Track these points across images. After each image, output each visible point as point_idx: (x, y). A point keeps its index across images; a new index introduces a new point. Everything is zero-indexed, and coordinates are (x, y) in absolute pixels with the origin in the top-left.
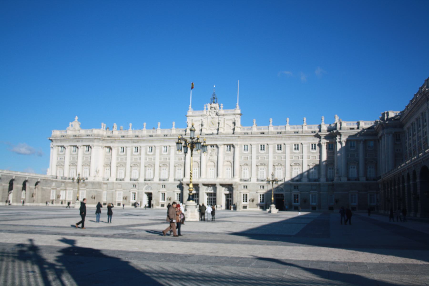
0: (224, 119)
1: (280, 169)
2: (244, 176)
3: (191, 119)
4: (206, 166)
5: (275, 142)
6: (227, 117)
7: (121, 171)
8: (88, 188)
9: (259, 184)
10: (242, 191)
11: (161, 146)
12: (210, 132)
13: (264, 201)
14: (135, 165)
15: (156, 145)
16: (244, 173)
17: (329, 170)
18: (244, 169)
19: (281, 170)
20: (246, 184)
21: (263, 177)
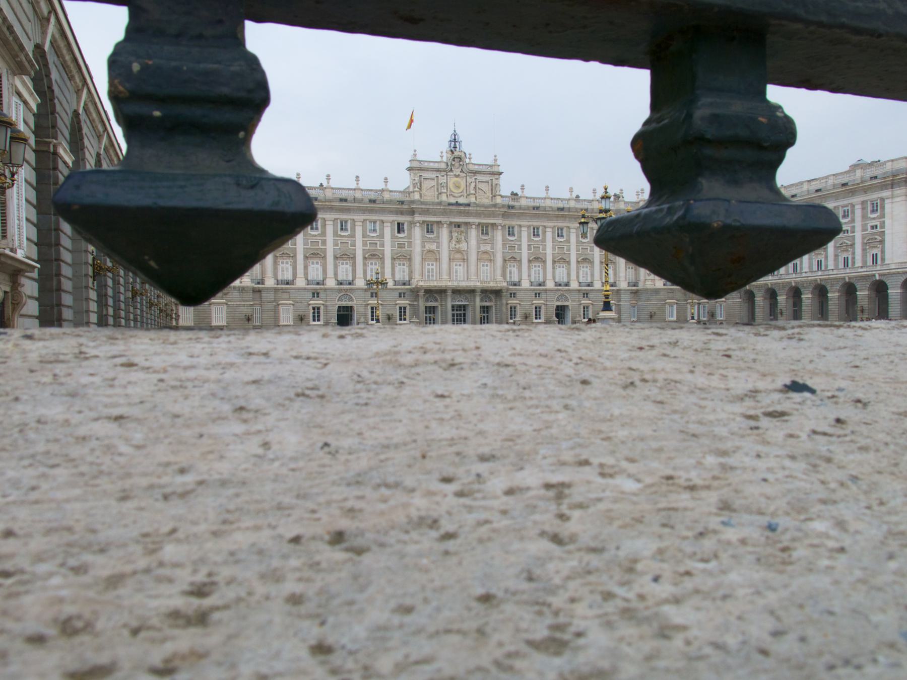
0: (476, 179)
1: (563, 267)
2: (510, 277)
3: (418, 175)
4: (450, 259)
5: (556, 224)
6: (480, 178)
7: (285, 265)
8: (230, 301)
9: (534, 290)
10: (509, 302)
11: (365, 220)
12: (453, 200)
13: (543, 316)
14: (315, 255)
15: (356, 217)
16: (510, 273)
17: (628, 270)
18: (510, 266)
19: (564, 269)
20: (515, 290)
21: (539, 280)
